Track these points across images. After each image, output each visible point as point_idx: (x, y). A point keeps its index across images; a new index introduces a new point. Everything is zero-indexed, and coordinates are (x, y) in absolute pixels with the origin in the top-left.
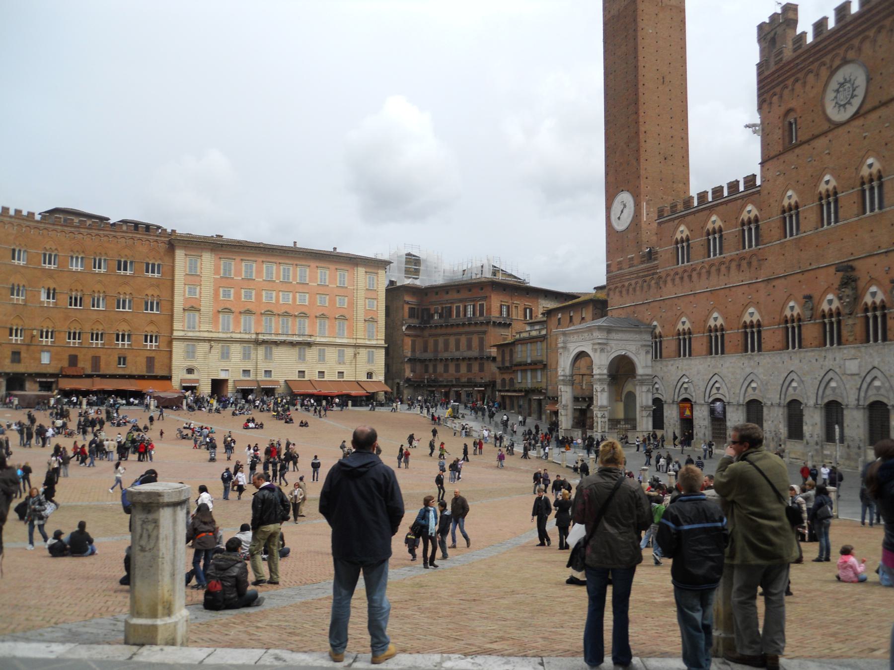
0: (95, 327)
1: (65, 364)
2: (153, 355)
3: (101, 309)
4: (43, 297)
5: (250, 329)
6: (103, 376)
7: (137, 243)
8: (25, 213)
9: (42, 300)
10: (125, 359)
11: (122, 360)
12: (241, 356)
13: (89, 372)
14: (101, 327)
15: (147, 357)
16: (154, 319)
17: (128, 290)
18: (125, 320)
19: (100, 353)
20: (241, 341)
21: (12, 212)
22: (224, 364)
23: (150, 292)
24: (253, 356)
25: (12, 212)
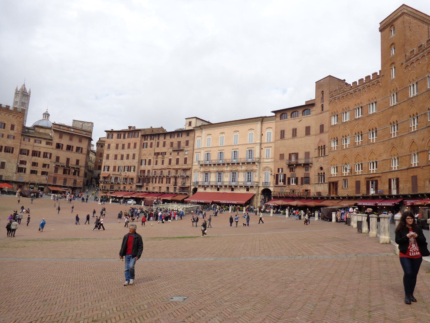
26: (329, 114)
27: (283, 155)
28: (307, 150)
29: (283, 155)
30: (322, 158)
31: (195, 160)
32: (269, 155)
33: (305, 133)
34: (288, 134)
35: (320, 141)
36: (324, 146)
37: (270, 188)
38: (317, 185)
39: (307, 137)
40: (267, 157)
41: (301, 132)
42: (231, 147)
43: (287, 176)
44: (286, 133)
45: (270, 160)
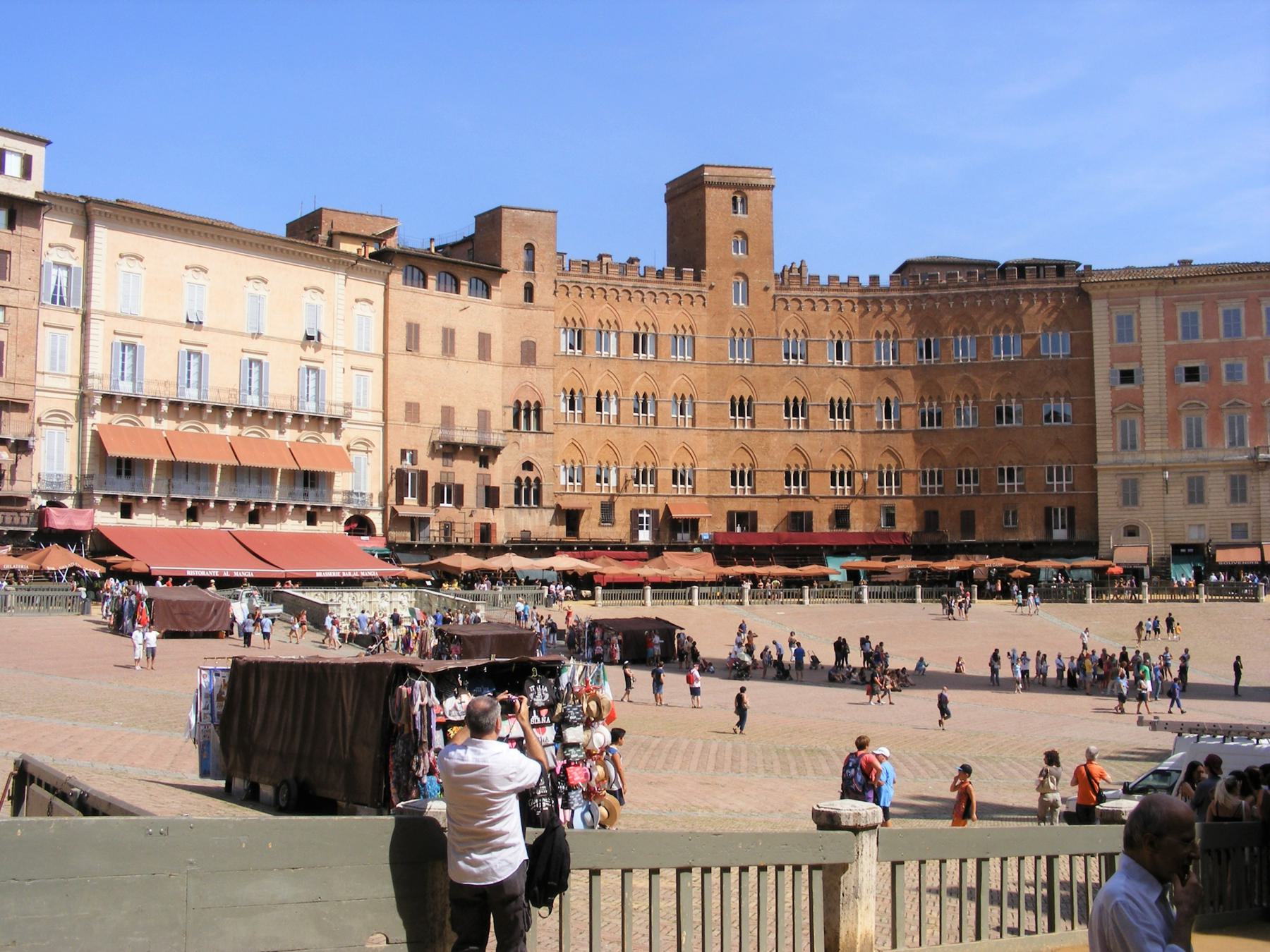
5: (1242, 442)
8: (844, 279)
12: (1226, 495)
20: (1226, 467)
21: (824, 281)
22: (1195, 511)
24: (1250, 494)
25: (824, 281)
26: (556, 319)
27: (417, 405)
28: (484, 406)
29: (417, 405)
30: (531, 438)
31: (44, 363)
32: (365, 400)
34: (431, 342)
36: (538, 403)
37: (370, 515)
38: (514, 511)
39: (483, 365)
40: (359, 404)
41: (467, 345)
42: (238, 338)
43: (432, 481)
44: (422, 336)
45: (369, 417)
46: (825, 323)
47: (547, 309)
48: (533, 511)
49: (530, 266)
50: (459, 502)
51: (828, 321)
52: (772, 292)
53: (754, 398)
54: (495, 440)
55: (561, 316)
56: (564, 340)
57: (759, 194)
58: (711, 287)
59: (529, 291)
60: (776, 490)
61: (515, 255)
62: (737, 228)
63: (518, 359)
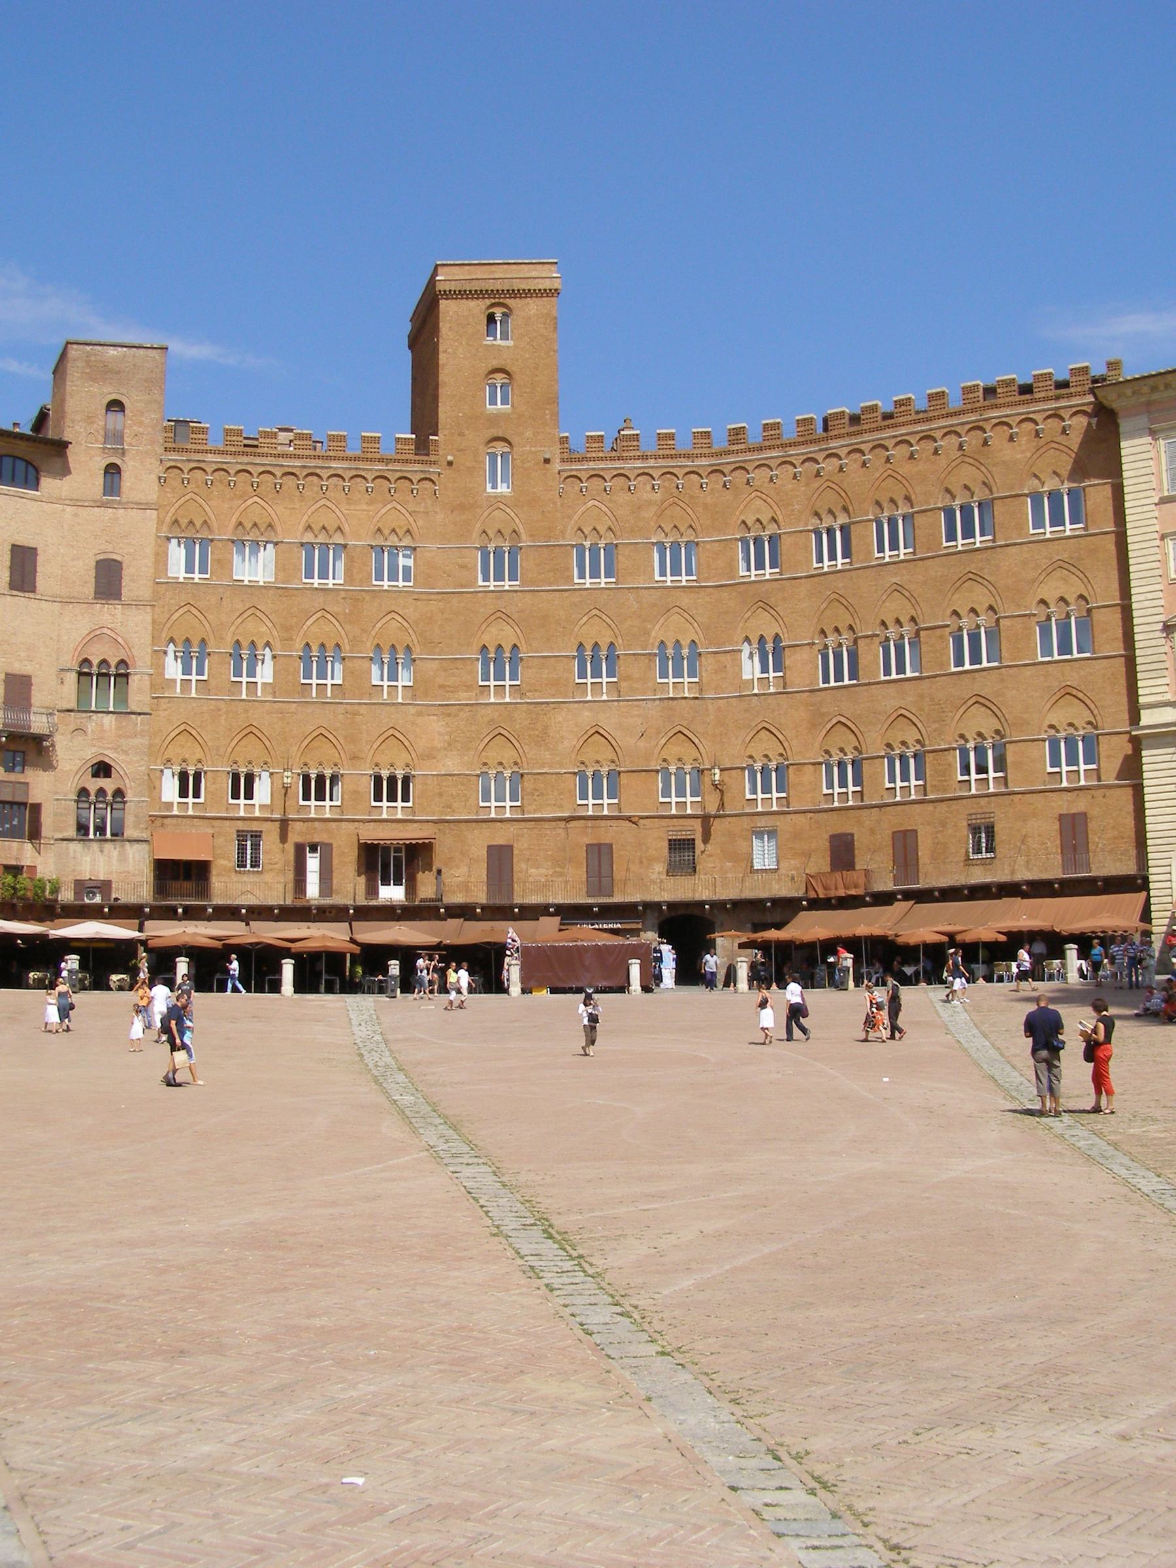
0: (896, 737)
1: (821, 863)
2: (1080, 805)
3: (909, 674)
4: (750, 669)
6: (922, 896)
7: (997, 438)
9: (746, 676)
10: (990, 830)
11: (984, 834)
13: (885, 884)
14: (911, 736)
15: (1061, 818)
16: (1072, 677)
17: (980, 597)
18: (981, 701)
19: (917, 819)
23: (1050, 590)
26: (160, 522)
28: (19, 668)
30: (108, 720)
33: (6, 576)
35: (94, 637)
39: (20, 601)
46: (649, 514)
47: (144, 507)
48: (108, 846)
49: (115, 438)
50: (35, 834)
51: (653, 509)
52: (557, 466)
53: (523, 647)
54: (38, 724)
55: (168, 520)
56: (177, 554)
57: (532, 307)
58: (450, 463)
59: (112, 471)
60: (561, 807)
61: (90, 420)
62: (495, 363)
63: (90, 589)
